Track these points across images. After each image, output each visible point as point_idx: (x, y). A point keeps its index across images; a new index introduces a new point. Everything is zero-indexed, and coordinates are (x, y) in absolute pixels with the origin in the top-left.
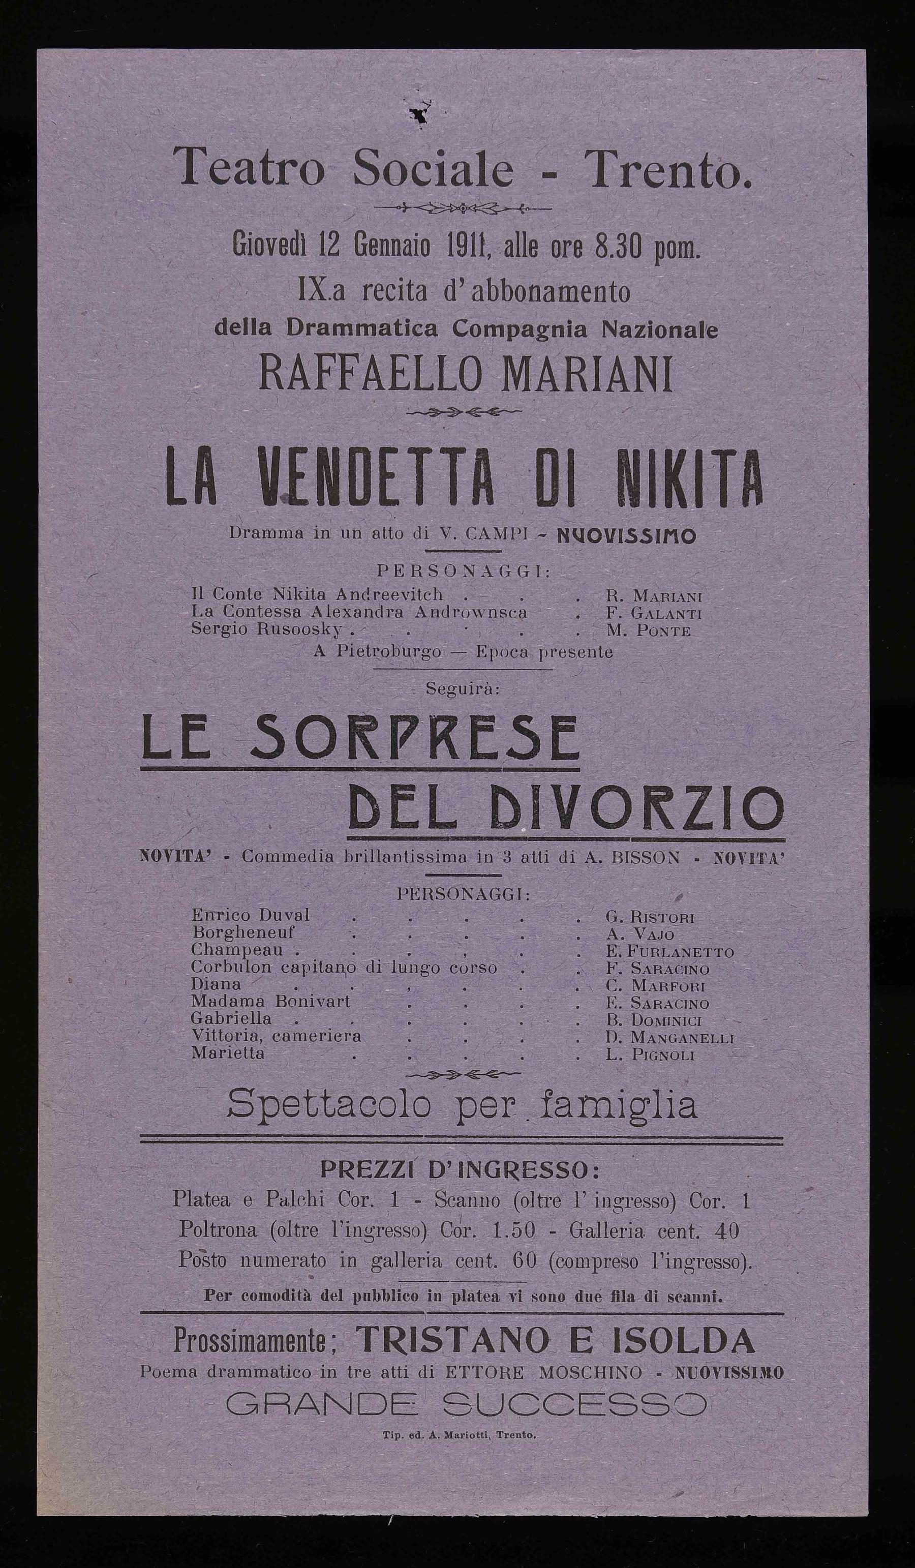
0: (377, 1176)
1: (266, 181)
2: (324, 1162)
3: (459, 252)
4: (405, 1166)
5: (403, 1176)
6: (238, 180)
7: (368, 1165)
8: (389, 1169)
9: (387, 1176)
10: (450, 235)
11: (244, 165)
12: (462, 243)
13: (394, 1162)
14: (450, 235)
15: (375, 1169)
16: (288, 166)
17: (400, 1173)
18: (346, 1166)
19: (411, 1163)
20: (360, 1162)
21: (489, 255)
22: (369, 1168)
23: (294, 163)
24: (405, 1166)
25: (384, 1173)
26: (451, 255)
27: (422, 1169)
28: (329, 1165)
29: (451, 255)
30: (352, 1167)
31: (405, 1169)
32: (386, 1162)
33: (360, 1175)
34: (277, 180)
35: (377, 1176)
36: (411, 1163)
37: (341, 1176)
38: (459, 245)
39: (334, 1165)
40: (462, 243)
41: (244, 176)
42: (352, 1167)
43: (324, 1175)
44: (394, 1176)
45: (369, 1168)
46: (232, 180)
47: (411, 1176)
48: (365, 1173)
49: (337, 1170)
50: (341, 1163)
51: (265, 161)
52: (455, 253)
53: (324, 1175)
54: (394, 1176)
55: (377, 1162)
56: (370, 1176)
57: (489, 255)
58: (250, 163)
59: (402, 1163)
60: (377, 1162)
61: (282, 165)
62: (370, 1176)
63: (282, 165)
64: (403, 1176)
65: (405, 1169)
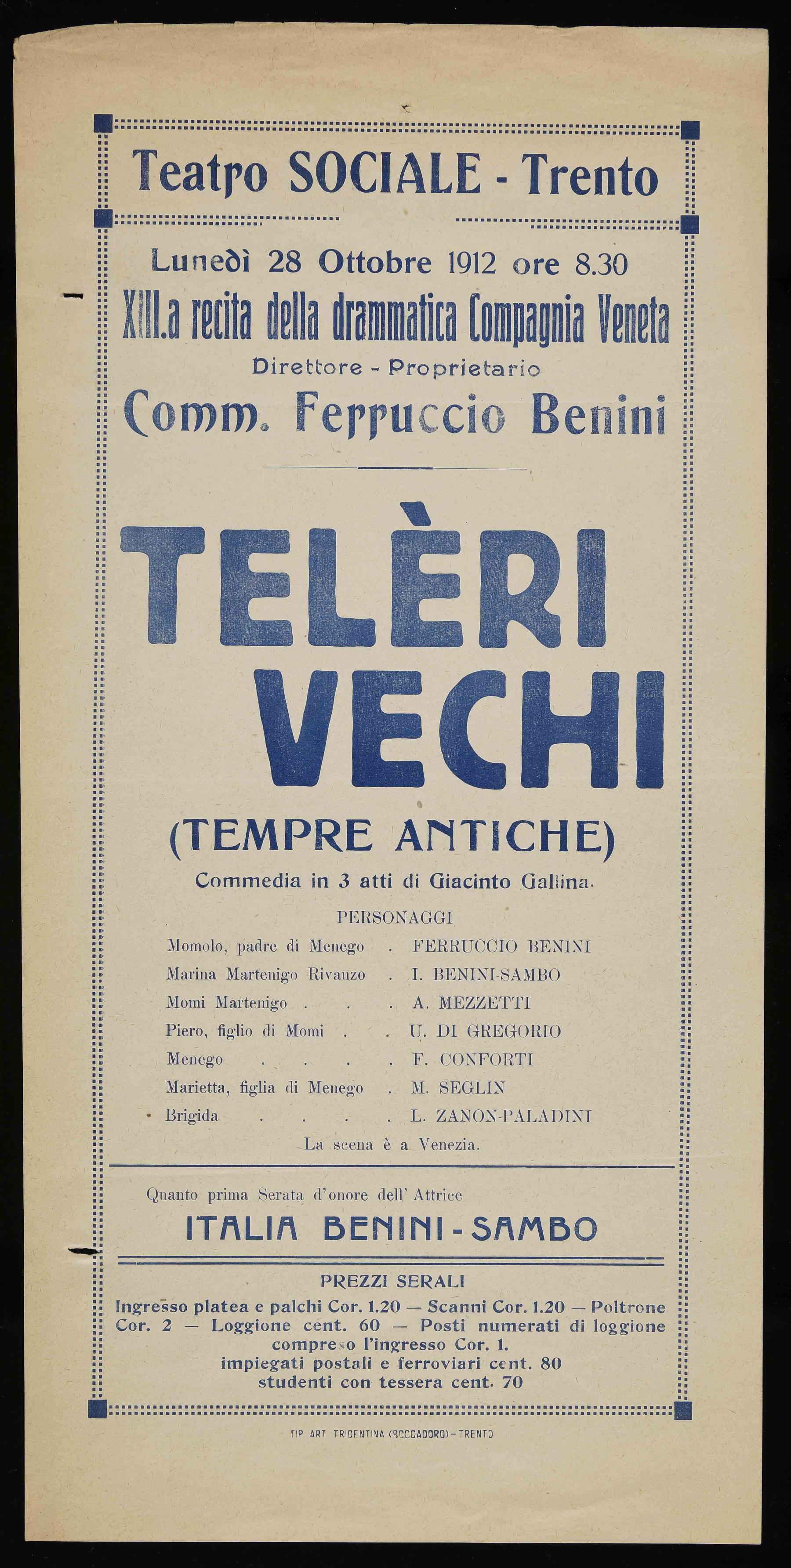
0: (362, 1286)
4: (382, 1279)
5: (380, 1286)
7: (355, 1278)
8: (370, 1281)
18: (339, 1279)
19: (385, 1276)
24: (382, 1279)
27: (392, 1281)
28: (326, 1279)
30: (343, 1279)
32: (367, 1277)
33: (349, 1285)
35: (362, 1286)
36: (385, 1276)
37: (336, 1286)
39: (330, 1279)
44: (373, 1286)
47: (385, 1286)
48: (353, 1284)
50: (336, 1276)
53: (323, 1286)
54: (373, 1286)
59: (379, 1276)
64: (380, 1286)
65: (381, 1281)
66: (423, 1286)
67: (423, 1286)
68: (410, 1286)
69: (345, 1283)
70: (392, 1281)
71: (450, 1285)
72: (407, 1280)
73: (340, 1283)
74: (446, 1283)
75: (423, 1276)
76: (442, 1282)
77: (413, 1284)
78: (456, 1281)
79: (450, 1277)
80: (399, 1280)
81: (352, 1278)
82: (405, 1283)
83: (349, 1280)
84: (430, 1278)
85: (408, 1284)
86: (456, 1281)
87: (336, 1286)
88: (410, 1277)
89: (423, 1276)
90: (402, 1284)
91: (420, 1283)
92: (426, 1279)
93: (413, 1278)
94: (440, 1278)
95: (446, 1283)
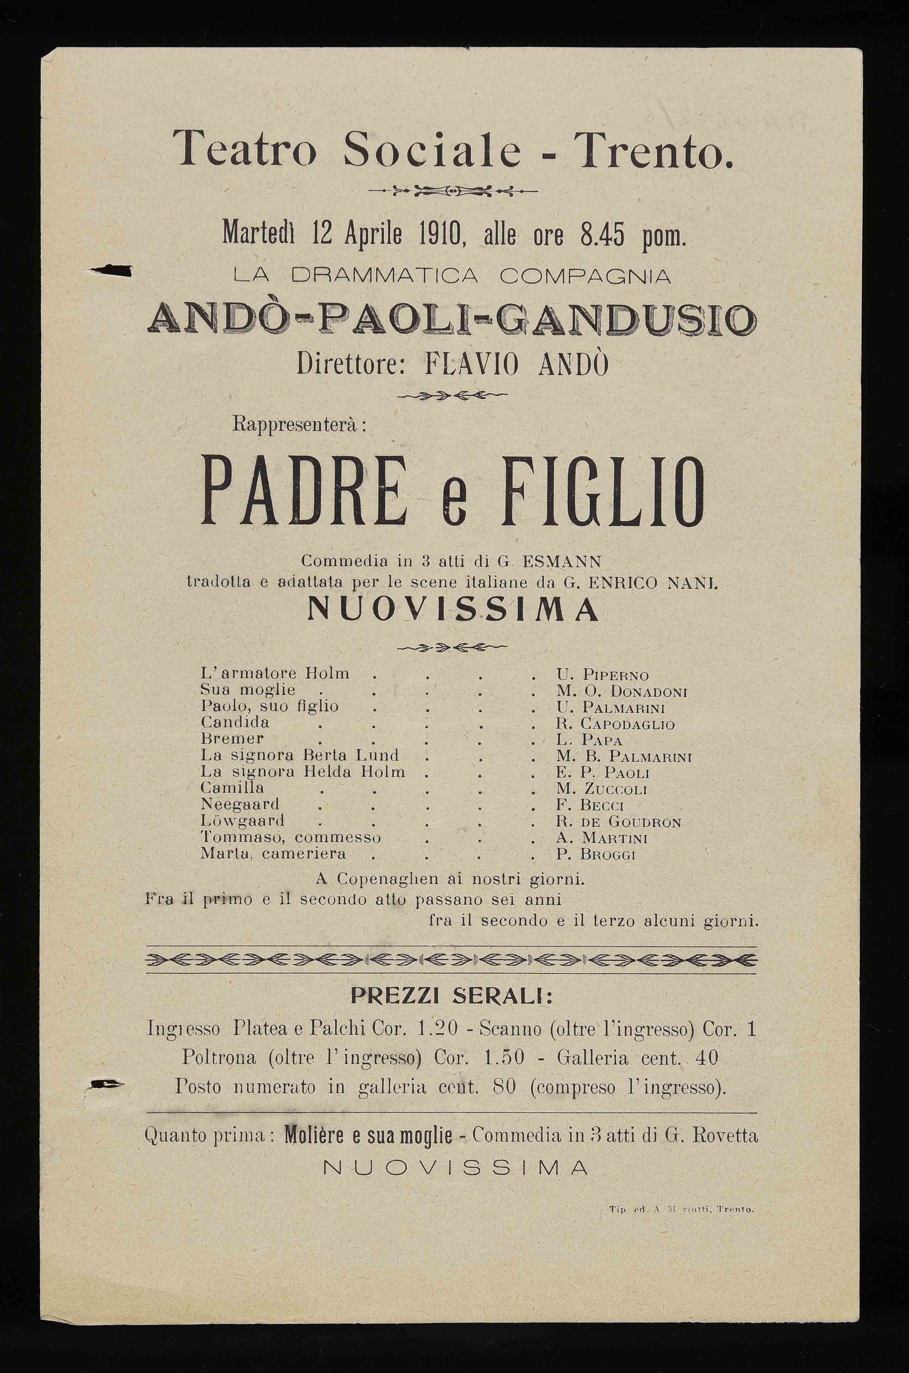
0: (405, 1001)
1: (261, 162)
2: (354, 989)
3: (430, 240)
4: (431, 994)
5: (429, 1002)
6: (234, 160)
8: (416, 995)
9: (413, 1002)
10: (422, 224)
11: (240, 147)
12: (434, 231)
13: (420, 988)
14: (422, 224)
15: (403, 995)
16: (282, 148)
17: (425, 1000)
18: (375, 993)
19: (436, 989)
20: (388, 989)
21: (464, 243)
22: (397, 995)
23: (287, 145)
24: (431, 994)
25: (410, 1000)
26: (423, 243)
27: (446, 995)
29: (423, 243)
30: (380, 993)
31: (430, 996)
32: (412, 989)
33: (388, 1001)
34: (272, 160)
36: (436, 989)
37: (370, 1002)
38: (431, 234)
40: (434, 231)
41: (240, 157)
42: (380, 993)
43: (354, 1002)
45: (397, 995)
46: (229, 162)
47: (436, 1001)
49: (366, 996)
50: (370, 989)
51: (260, 144)
52: (426, 240)
53: (354, 1002)
54: (421, 1001)
55: (405, 988)
56: (398, 1002)
57: (464, 243)
58: (246, 146)
59: (428, 989)
60: (405, 988)
61: (276, 147)
62: (398, 1002)
63: (276, 147)
64: (429, 1002)
65: (430, 996)
66: (488, 1002)
67: (488, 1002)
68: (471, 1001)
69: (382, 999)
70: (446, 995)
71: (523, 1002)
72: (467, 994)
73: (376, 998)
74: (518, 998)
75: (488, 989)
76: (513, 997)
77: (475, 999)
78: (531, 995)
79: (523, 990)
80: (456, 993)
81: (392, 991)
82: (464, 997)
83: (388, 994)
84: (498, 992)
85: (468, 999)
86: (531, 995)
87: (370, 1002)
88: (471, 989)
89: (488, 989)
90: (460, 999)
91: (484, 998)
92: (493, 993)
93: (475, 991)
94: (510, 991)
95: (518, 998)
